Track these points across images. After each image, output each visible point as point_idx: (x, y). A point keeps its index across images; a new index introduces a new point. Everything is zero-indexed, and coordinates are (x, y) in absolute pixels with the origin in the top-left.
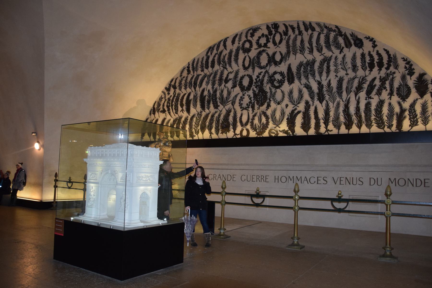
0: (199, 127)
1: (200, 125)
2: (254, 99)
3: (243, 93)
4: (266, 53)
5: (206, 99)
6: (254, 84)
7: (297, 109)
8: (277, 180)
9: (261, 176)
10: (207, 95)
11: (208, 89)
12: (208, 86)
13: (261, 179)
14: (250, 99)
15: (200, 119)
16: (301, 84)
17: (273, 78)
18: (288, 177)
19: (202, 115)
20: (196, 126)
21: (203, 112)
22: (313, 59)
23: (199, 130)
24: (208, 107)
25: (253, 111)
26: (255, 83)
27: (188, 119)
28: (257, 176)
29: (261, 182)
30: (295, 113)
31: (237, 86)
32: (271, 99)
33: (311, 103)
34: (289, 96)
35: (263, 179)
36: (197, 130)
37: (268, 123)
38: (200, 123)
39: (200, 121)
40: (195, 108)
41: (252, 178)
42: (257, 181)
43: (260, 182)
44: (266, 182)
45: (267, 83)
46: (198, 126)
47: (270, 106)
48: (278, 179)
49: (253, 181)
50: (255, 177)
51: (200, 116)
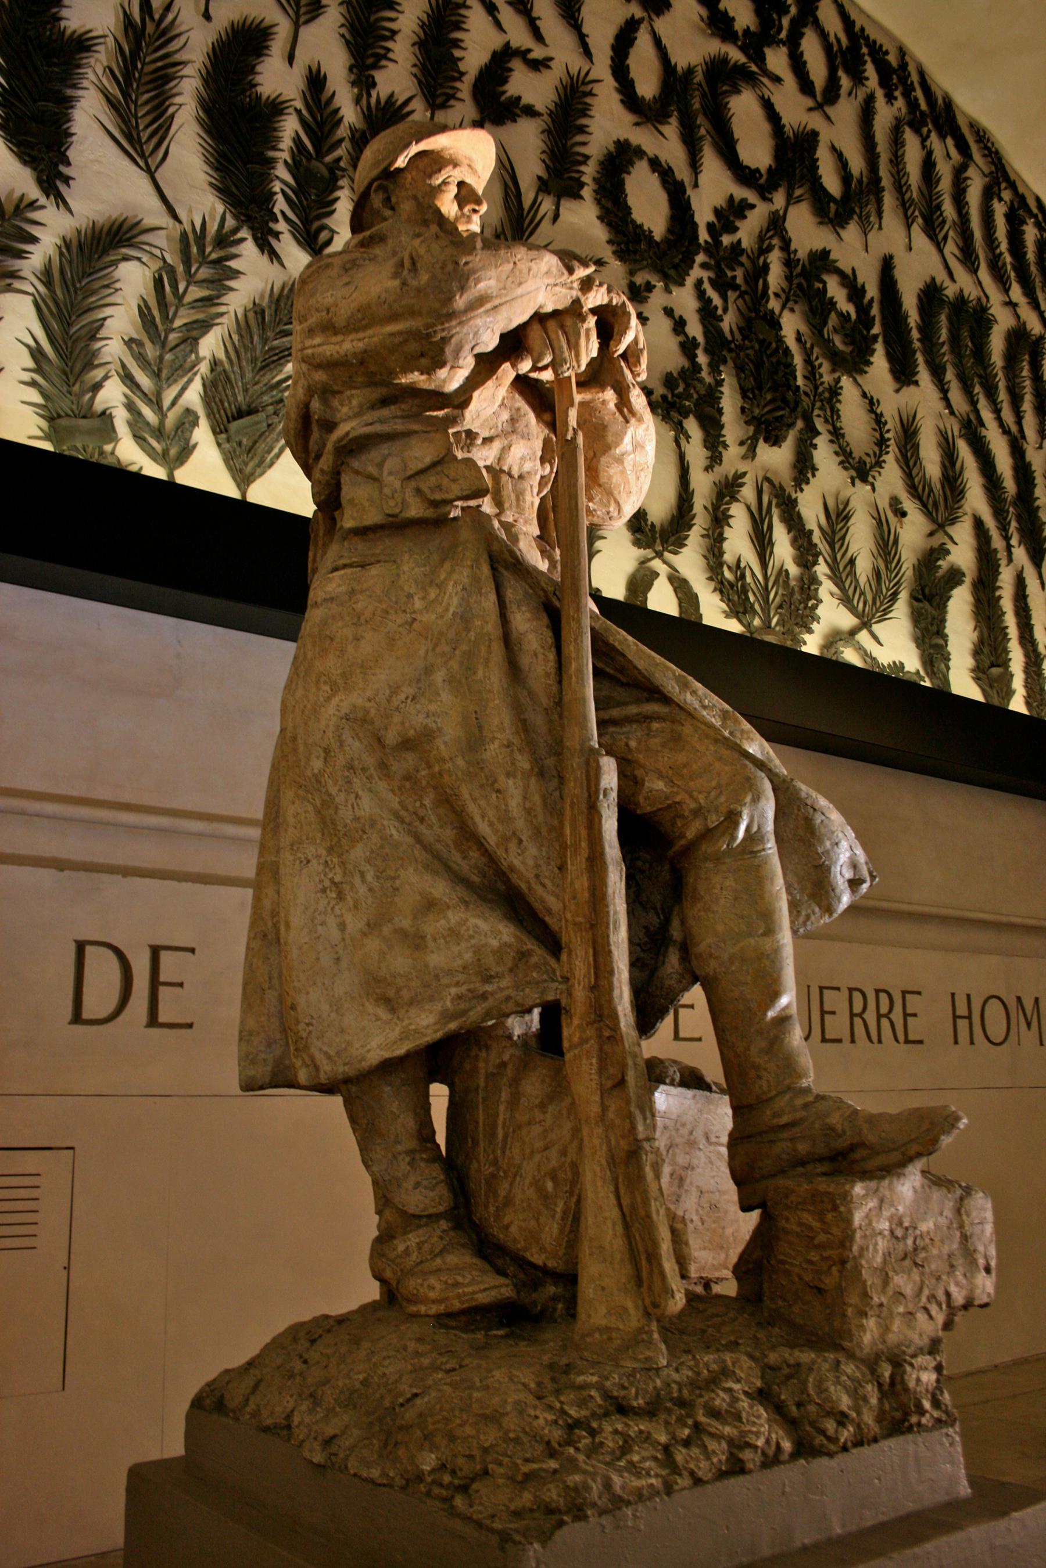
0: (193, 396)
1: (204, 368)
2: (714, 368)
3: (632, 273)
4: (762, 98)
5: (286, 143)
6: (700, 258)
7: (948, 552)
8: (962, 1024)
9: (877, 992)
10: (299, 104)
11: (303, 57)
12: (307, 33)
13: (879, 1016)
14: (688, 347)
15: (208, 301)
16: (952, 413)
17: (821, 286)
18: (1012, 1004)
19: (236, 274)
20: (151, 351)
21: (249, 249)
22: (979, 299)
23: (189, 420)
24: (306, 221)
25: (715, 459)
26: (708, 249)
27: (34, 240)
28: (851, 990)
29: (880, 1041)
30: (940, 573)
31: (587, 192)
32: (819, 424)
33: (997, 542)
34: (904, 455)
35: (886, 1016)
36: (172, 417)
37: (808, 586)
38: (210, 345)
39: (204, 326)
40: (142, 156)
41: (823, 1012)
42: (853, 1041)
43: (876, 1045)
44: (907, 1041)
45: (787, 298)
46: (183, 369)
47: (814, 469)
48: (969, 1017)
49: (827, 1037)
50: (836, 1001)
51: (204, 273)
